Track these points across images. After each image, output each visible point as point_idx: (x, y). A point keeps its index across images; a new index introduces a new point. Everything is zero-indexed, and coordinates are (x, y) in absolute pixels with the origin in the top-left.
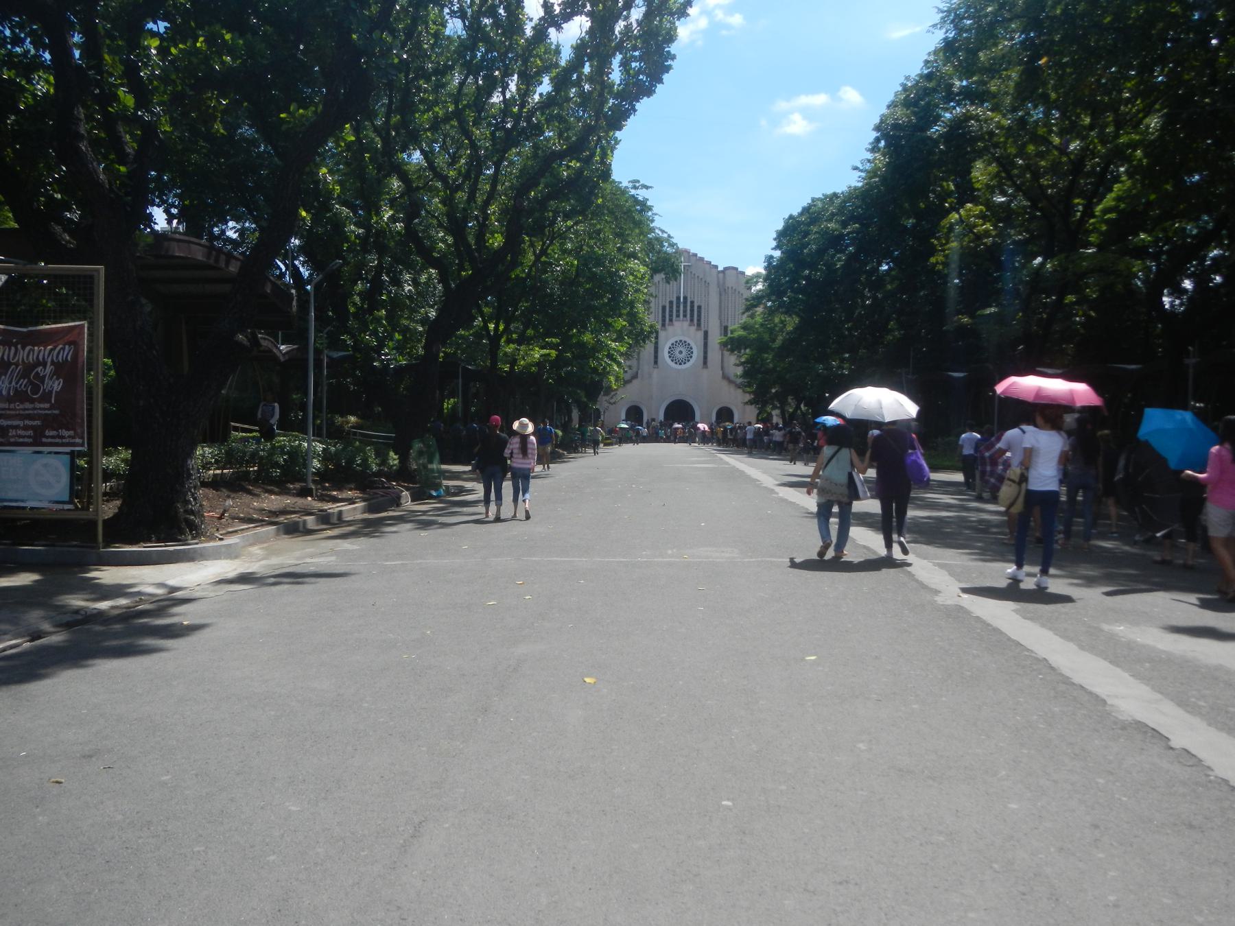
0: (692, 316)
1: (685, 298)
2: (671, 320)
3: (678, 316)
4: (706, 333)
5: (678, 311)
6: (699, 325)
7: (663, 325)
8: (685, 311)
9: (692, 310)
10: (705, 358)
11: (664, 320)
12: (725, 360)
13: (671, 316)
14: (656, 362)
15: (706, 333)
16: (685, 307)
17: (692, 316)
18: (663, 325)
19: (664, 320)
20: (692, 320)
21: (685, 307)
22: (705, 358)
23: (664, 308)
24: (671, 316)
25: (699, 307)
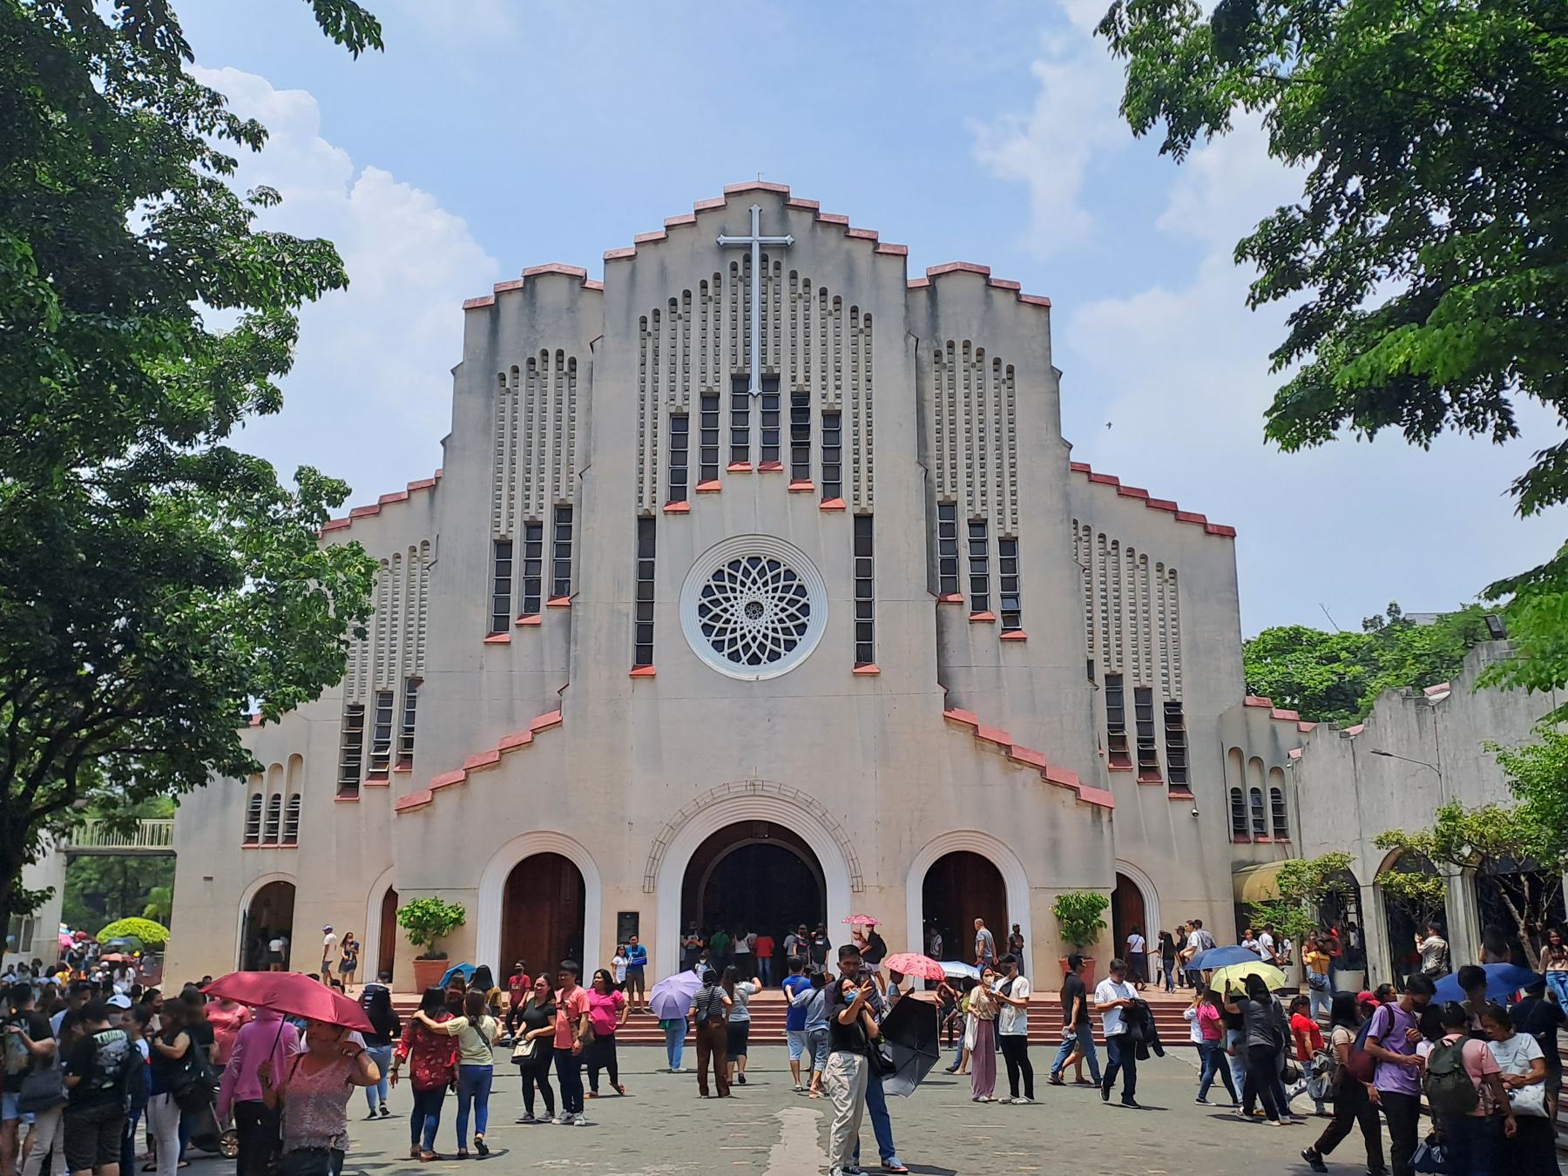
0: (801, 447)
1: (770, 381)
2: (709, 472)
3: (740, 453)
4: (864, 522)
5: (740, 434)
6: (832, 488)
7: (678, 493)
8: (770, 437)
9: (801, 430)
10: (864, 631)
11: (678, 477)
12: (953, 638)
13: (709, 453)
14: (644, 655)
15: (864, 522)
16: (770, 415)
17: (801, 447)
18: (678, 493)
19: (678, 477)
20: (800, 470)
21: (770, 415)
22: (864, 631)
23: (679, 421)
24: (709, 453)
25: (832, 418)
